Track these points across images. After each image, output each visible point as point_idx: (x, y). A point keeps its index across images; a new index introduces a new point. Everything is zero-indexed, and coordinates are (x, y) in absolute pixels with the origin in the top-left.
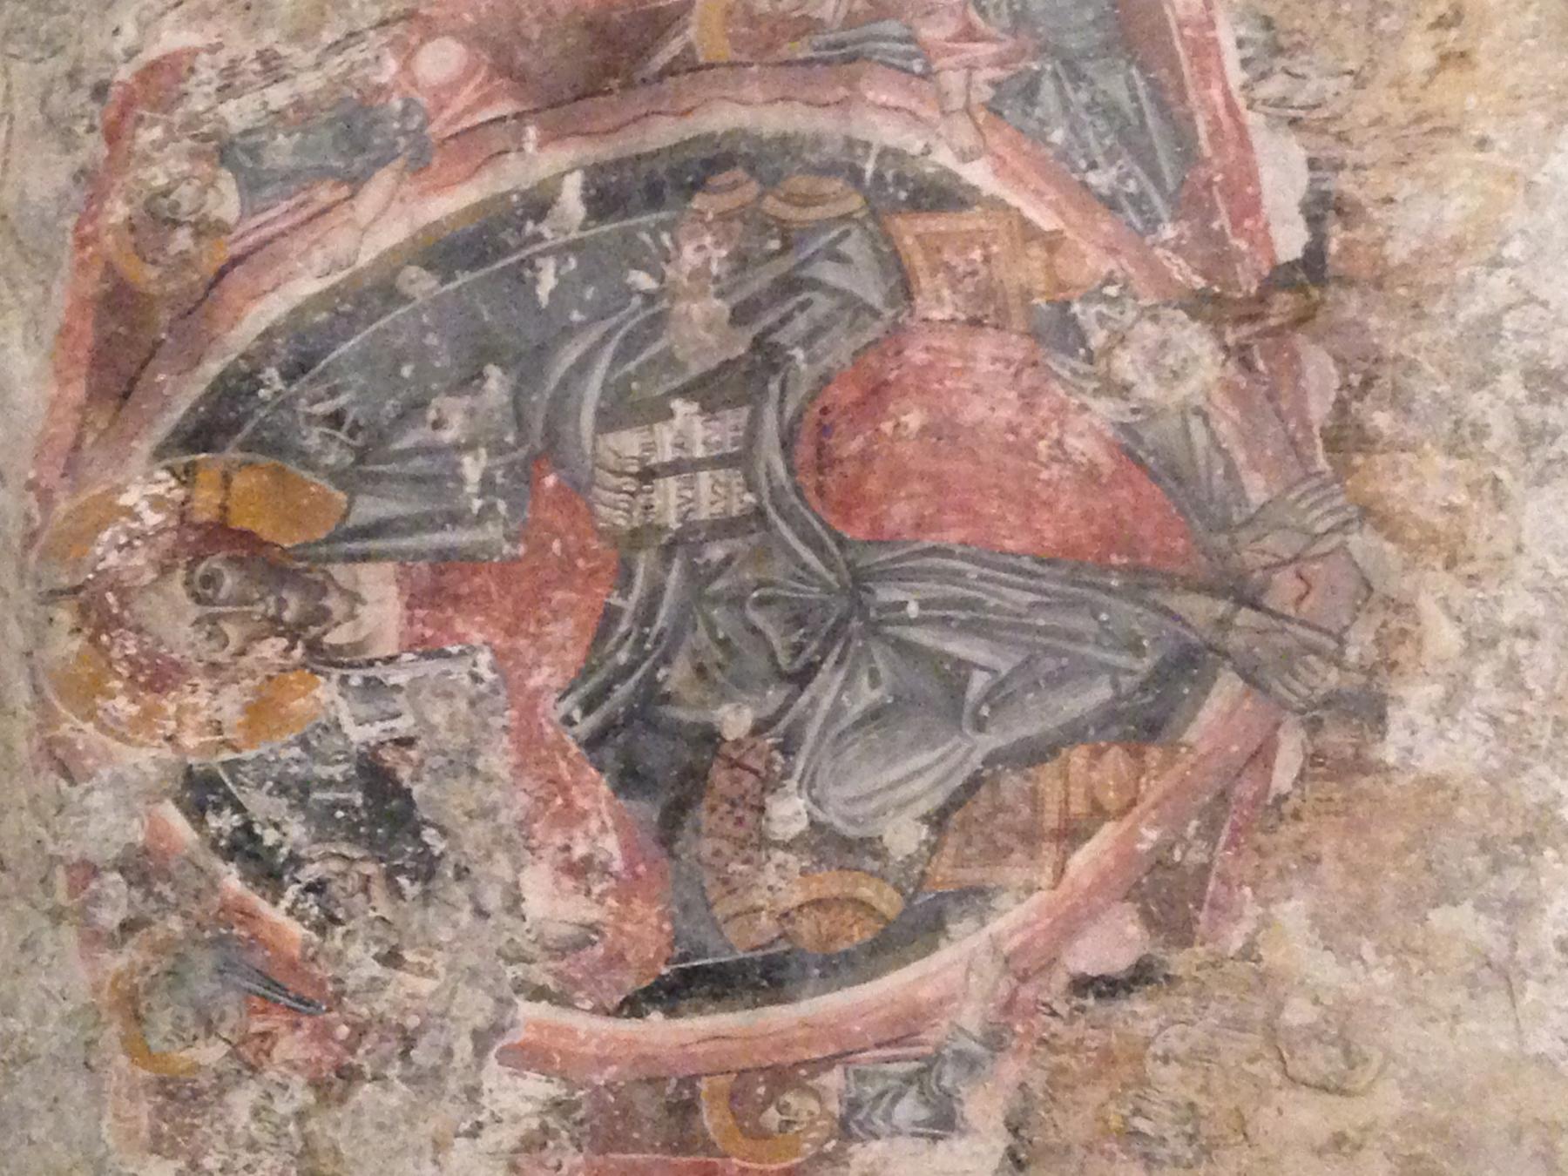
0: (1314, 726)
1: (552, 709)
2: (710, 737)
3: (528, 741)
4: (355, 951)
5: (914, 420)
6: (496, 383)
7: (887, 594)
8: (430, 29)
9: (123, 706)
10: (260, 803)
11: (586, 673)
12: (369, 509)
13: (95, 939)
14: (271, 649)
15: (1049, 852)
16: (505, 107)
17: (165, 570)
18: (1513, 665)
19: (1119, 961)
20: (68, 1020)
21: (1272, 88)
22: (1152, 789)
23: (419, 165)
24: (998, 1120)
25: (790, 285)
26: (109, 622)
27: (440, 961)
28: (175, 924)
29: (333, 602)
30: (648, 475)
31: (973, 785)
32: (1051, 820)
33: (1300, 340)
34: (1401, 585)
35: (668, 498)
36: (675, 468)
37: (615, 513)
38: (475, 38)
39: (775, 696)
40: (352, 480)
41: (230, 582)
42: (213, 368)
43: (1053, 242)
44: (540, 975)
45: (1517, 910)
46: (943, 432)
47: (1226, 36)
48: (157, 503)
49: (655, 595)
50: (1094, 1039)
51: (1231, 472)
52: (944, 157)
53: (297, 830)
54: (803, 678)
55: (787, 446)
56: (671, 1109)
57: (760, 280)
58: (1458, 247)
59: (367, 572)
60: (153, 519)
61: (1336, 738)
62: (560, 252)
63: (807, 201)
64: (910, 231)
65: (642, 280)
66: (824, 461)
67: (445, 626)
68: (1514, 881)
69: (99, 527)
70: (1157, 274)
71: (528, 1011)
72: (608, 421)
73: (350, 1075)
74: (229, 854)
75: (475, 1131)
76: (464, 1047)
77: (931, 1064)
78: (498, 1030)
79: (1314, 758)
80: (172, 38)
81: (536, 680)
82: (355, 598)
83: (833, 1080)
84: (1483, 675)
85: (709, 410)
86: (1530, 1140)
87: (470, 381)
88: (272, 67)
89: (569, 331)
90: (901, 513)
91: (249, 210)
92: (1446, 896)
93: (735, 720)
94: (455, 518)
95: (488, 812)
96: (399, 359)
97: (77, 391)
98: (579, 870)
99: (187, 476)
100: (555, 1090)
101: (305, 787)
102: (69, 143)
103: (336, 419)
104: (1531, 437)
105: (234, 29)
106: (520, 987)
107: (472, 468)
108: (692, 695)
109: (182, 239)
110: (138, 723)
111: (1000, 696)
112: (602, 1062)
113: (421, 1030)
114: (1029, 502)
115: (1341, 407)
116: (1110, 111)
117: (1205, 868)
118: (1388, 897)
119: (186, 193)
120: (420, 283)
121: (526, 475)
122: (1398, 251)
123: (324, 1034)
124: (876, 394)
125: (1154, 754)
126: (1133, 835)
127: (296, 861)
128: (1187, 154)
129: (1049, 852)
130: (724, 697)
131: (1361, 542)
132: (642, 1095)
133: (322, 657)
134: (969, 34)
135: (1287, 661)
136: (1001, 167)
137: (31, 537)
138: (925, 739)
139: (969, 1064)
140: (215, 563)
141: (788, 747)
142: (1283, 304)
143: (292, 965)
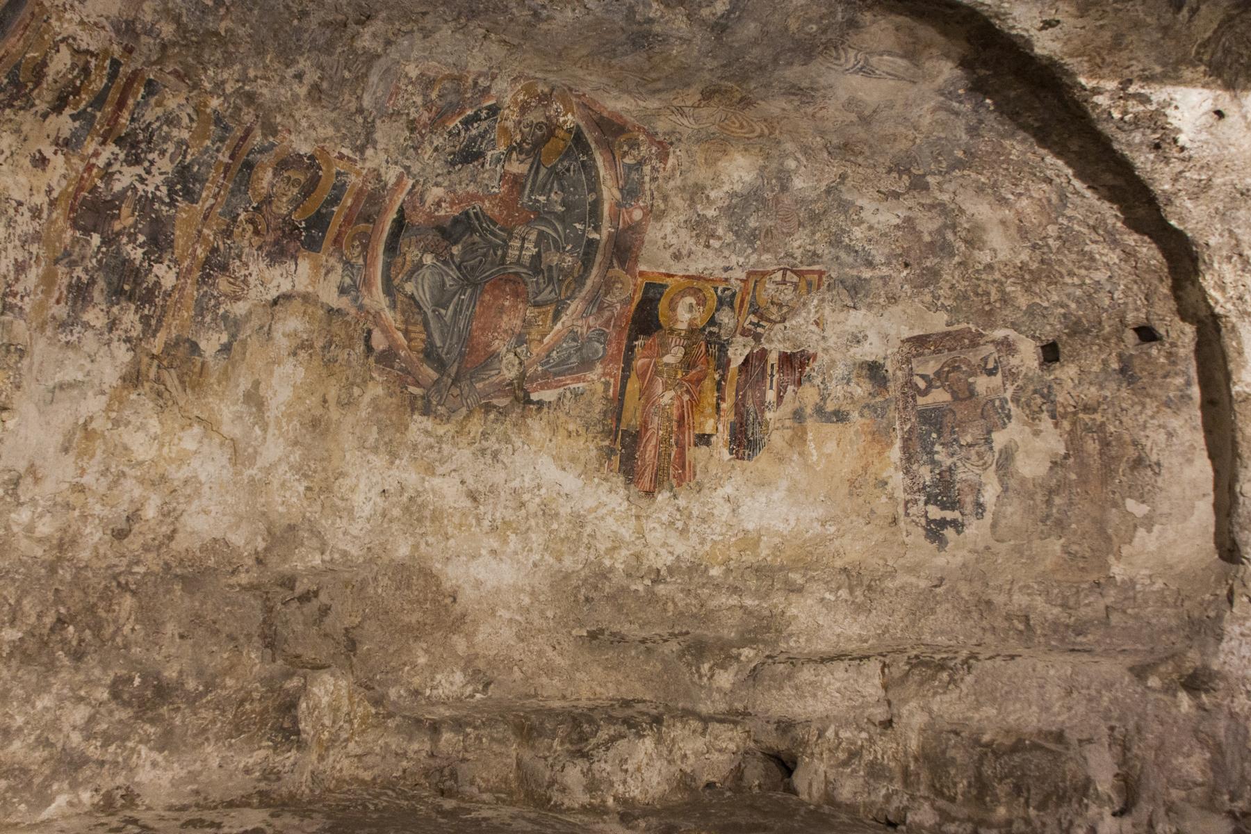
0: (423, 397)
1: (478, 204)
2: (456, 243)
3: (474, 197)
4: (441, 140)
5: (507, 303)
6: (560, 209)
7: (469, 291)
8: (645, 215)
9: (521, 97)
10: (484, 125)
11: (484, 215)
12: (543, 171)
13: (480, 75)
14: (518, 138)
15: (403, 327)
16: (621, 226)
17: (547, 118)
18: (432, 447)
19: (374, 343)
20: (467, 63)
21: (568, 394)
22: (414, 355)
23: (618, 204)
24: (342, 306)
25: (550, 280)
26: (540, 100)
27: (431, 162)
28: (469, 95)
29: (523, 156)
30: (524, 239)
31: (420, 308)
32: (411, 328)
33: (511, 398)
34: (455, 418)
35: (516, 243)
36: (522, 247)
37: (520, 230)
38: (639, 223)
39: (457, 260)
40: (552, 170)
41: (539, 133)
42: (593, 146)
43: (541, 341)
44: (419, 188)
45: (375, 450)
46: (501, 310)
47: (581, 385)
48: (565, 122)
49: (495, 235)
50: (356, 336)
51: (484, 379)
52: (564, 318)
53: (474, 132)
54: (459, 268)
55: (517, 274)
56: (369, 216)
57: (555, 274)
58: (529, 435)
59: (528, 166)
60: (561, 119)
61: (419, 403)
62: (584, 231)
63: (567, 287)
64: (551, 309)
65: (568, 248)
66: (507, 281)
67: (507, 182)
68: (382, 449)
69: (565, 106)
70: (531, 365)
71: (411, 182)
72: (541, 234)
73: (412, 130)
74: (476, 113)
75: (387, 162)
76: (408, 163)
77: (358, 290)
78: (409, 173)
79: (415, 397)
80: (671, 161)
81: (487, 203)
82: (522, 162)
83: (361, 261)
84: (431, 440)
85: (533, 256)
86: (326, 454)
87: (563, 203)
88: (654, 179)
89: (565, 229)
90: (487, 297)
91: (625, 165)
92: (380, 431)
93: (456, 250)
94: (532, 191)
95: (460, 184)
96: (575, 188)
97: (605, 114)
98: (438, 204)
99: (569, 131)
100: (390, 186)
101: (483, 137)
102: (665, 134)
103: (568, 170)
104: (483, 451)
105: (667, 174)
106: (417, 182)
107: (542, 199)
108: (470, 241)
109: (626, 148)
110: (516, 100)
111: (440, 317)
112: (391, 200)
113: (417, 153)
114: (483, 329)
115: (495, 407)
116: (569, 357)
117: (393, 367)
118: (381, 415)
119: (636, 153)
120: (591, 198)
121: (536, 211)
122: (529, 421)
123: (425, 126)
124: (516, 295)
125: (421, 356)
126: (404, 349)
127: (467, 130)
128: (556, 375)
129: (403, 327)
130: (463, 248)
131: (464, 411)
132: (377, 208)
133: (511, 150)
134: (589, 327)
135: (438, 391)
136: (559, 331)
137: (571, 90)
138: (433, 296)
139: (356, 299)
140: (545, 130)
141: (445, 262)
142: (521, 394)
143: (444, 122)
